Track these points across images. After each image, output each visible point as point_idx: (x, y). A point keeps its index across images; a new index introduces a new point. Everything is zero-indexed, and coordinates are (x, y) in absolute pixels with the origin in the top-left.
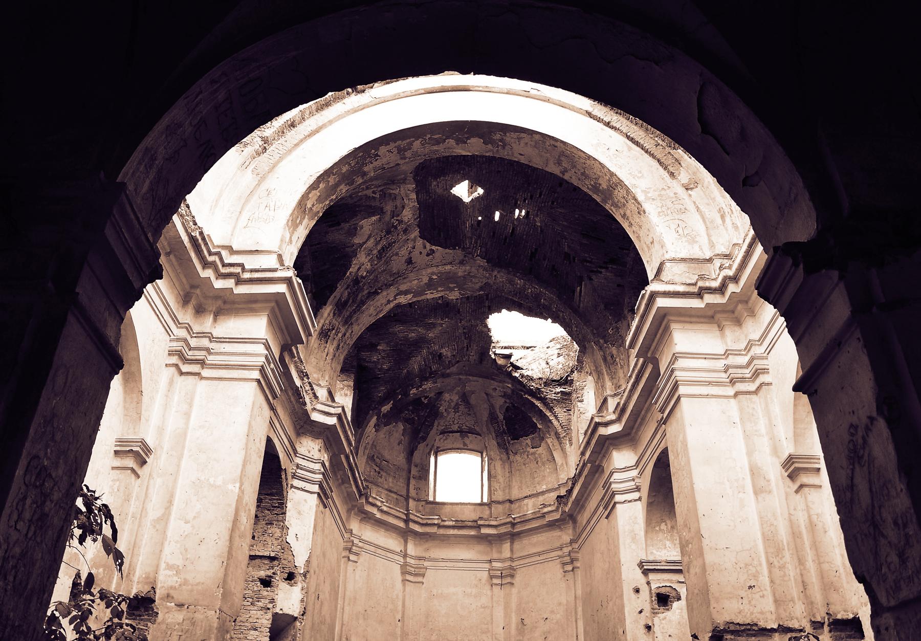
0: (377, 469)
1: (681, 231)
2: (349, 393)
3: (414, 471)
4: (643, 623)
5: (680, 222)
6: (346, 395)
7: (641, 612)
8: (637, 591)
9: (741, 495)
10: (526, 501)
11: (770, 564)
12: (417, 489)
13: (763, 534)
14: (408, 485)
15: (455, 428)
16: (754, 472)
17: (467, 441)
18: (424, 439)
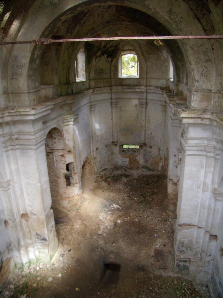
0: (99, 73)
1: (203, 74)
2: (83, 54)
3: (113, 69)
4: (175, 165)
5: (205, 70)
6: (82, 55)
7: (175, 162)
8: (175, 155)
9: (198, 189)
10: (152, 80)
11: (200, 212)
12: (114, 74)
13: (201, 203)
14: (111, 74)
15: (127, 49)
16: (205, 184)
17: (131, 52)
18: (115, 57)
